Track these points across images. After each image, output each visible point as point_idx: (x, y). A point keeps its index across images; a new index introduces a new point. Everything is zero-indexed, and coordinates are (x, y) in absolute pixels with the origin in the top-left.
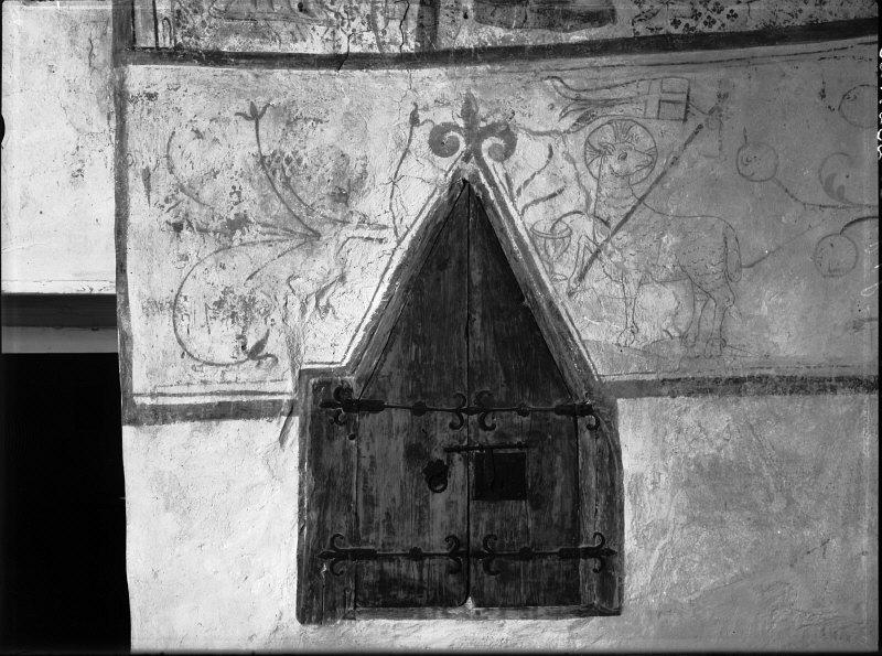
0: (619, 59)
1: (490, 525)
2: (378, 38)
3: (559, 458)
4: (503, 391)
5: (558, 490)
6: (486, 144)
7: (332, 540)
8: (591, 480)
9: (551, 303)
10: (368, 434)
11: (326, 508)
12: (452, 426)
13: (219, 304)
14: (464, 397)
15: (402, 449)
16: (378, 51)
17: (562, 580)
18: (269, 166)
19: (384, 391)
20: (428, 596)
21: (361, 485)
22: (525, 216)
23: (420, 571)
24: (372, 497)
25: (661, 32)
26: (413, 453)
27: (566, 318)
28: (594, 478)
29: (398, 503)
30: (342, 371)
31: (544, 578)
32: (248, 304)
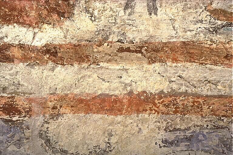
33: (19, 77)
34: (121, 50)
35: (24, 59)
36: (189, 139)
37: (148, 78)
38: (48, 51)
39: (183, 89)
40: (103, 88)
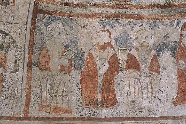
2: (13, 113)
16: (13, 116)
33: (72, 9)
34: (91, 5)
35: (73, 6)
36: (103, 22)
37: (96, 11)
38: (77, 5)
39: (102, 13)
40: (87, 12)
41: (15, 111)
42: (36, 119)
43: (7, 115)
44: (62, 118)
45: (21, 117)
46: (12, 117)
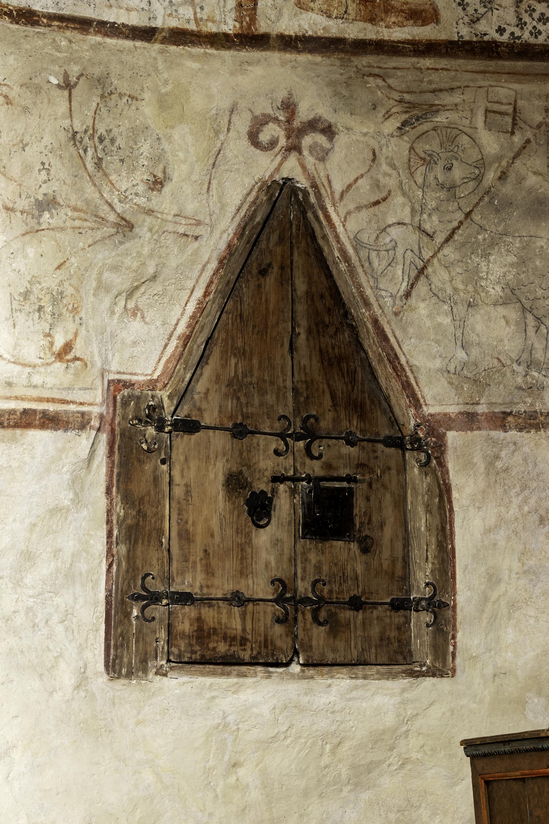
0: (443, 63)
1: (318, 568)
2: (195, 14)
3: (388, 496)
4: (329, 416)
5: (388, 532)
6: (307, 141)
7: (144, 579)
8: (421, 521)
9: (376, 322)
10: (182, 458)
11: (136, 542)
12: (277, 453)
13: (26, 295)
14: (289, 420)
15: (221, 478)
17: (393, 634)
18: (81, 142)
19: (199, 409)
20: (252, 649)
21: (175, 517)
22: (346, 225)
23: (243, 619)
24: (187, 531)
25: (486, 38)
26: (235, 482)
27: (392, 340)
28: (423, 521)
29: (217, 539)
30: (152, 384)
31: (375, 631)
32: (57, 298)
41: (202, 8)
42: (289, 43)
43: (173, 23)
44: (399, 42)
45: (226, 35)
46: (192, 34)
